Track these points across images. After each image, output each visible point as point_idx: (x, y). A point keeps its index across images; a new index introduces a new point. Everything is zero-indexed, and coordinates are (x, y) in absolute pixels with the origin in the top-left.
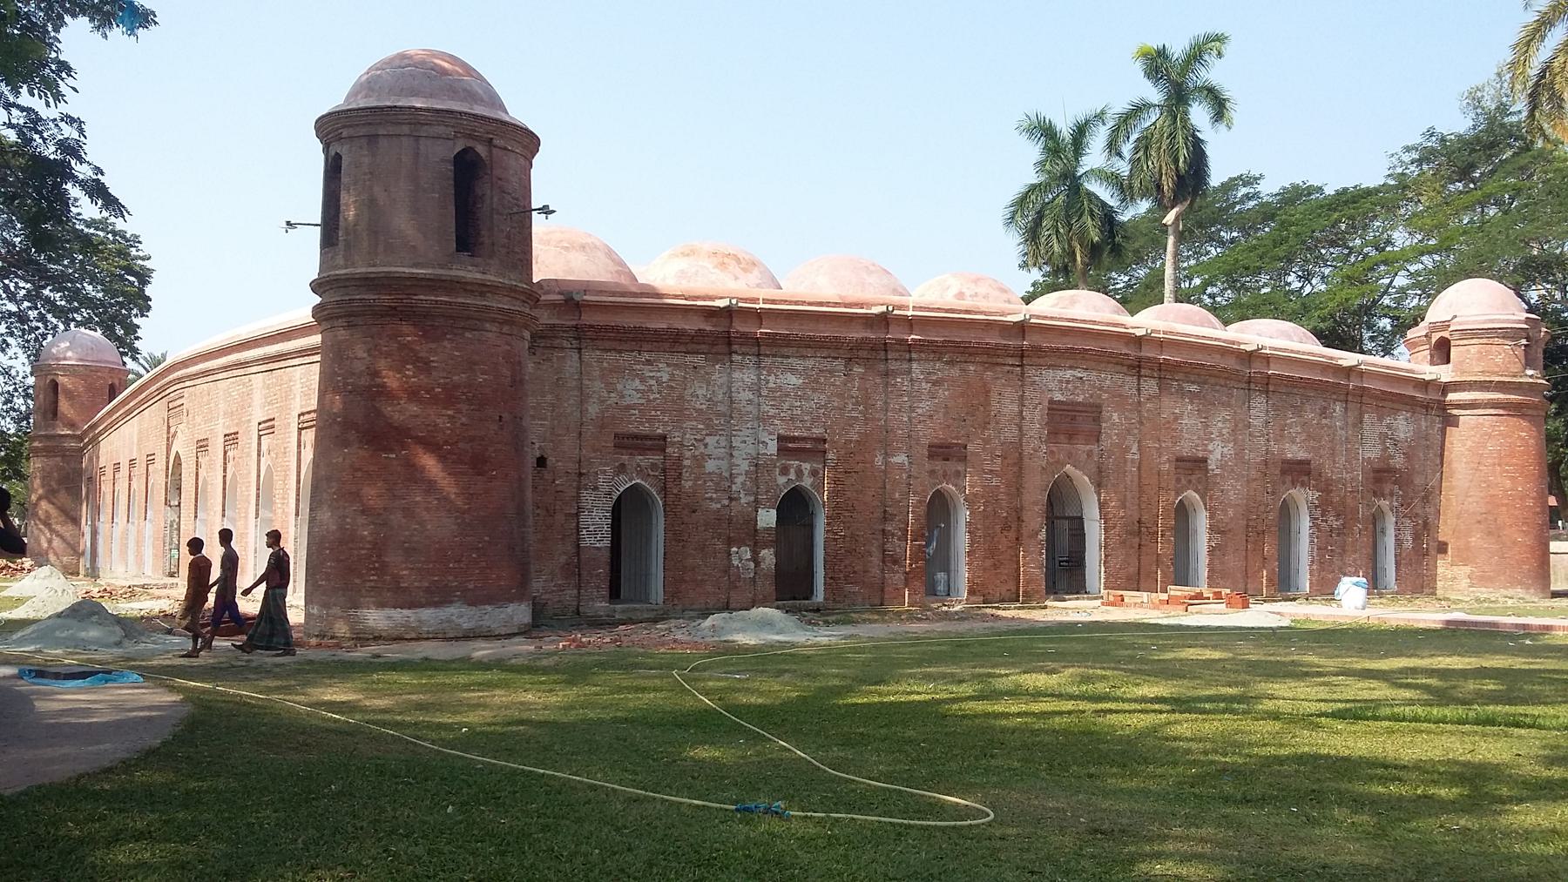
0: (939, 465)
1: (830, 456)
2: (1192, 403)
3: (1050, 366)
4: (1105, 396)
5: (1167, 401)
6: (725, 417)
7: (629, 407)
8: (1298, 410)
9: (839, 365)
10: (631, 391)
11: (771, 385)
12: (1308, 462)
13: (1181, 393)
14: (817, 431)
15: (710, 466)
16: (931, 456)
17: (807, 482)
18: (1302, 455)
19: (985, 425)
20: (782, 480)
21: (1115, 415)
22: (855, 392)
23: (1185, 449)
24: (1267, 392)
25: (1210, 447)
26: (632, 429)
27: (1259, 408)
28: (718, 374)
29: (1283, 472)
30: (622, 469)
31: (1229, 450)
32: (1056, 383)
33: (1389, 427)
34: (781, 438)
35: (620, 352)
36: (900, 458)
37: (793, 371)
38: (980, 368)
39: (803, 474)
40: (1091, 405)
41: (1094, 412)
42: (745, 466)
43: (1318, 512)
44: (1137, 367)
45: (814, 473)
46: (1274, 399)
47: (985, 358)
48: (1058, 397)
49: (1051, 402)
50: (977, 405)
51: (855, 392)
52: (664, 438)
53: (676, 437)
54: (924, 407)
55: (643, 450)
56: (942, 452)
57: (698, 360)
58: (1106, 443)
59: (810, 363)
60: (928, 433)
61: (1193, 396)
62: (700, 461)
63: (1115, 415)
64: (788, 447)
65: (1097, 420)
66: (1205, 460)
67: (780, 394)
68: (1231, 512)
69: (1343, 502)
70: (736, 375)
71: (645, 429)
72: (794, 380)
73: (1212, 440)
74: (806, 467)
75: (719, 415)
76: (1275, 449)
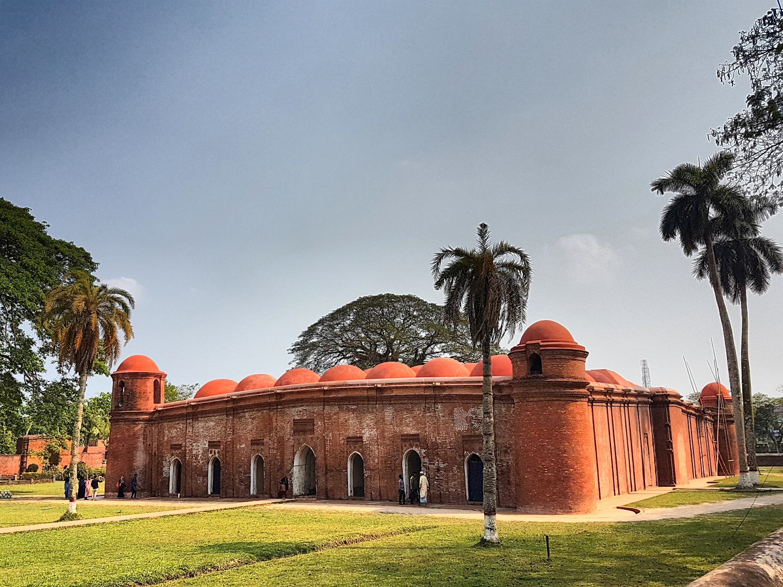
0: (255, 447)
1: (221, 447)
2: (353, 413)
3: (293, 407)
4: (315, 415)
5: (341, 414)
7: (174, 437)
8: (410, 411)
10: (174, 432)
11: (207, 426)
13: (348, 410)
16: (252, 444)
17: (217, 455)
18: (413, 432)
19: (270, 431)
20: (210, 455)
21: (319, 422)
22: (230, 425)
23: (351, 433)
24: (392, 404)
25: (363, 432)
26: (174, 443)
27: (389, 413)
30: (172, 455)
32: (295, 413)
33: (474, 413)
34: (209, 442)
35: (172, 422)
36: (243, 446)
37: (212, 421)
38: (268, 411)
39: (216, 453)
40: (309, 419)
41: (311, 421)
43: (426, 460)
44: (325, 402)
49: (294, 420)
50: (268, 426)
51: (230, 425)
52: (181, 444)
54: (250, 427)
55: (178, 449)
56: (254, 442)
58: (316, 434)
60: (250, 437)
61: (354, 411)
63: (319, 422)
64: (212, 444)
66: (361, 437)
67: (208, 429)
68: (376, 461)
71: (177, 443)
72: (213, 424)
74: (217, 450)
75: (197, 436)
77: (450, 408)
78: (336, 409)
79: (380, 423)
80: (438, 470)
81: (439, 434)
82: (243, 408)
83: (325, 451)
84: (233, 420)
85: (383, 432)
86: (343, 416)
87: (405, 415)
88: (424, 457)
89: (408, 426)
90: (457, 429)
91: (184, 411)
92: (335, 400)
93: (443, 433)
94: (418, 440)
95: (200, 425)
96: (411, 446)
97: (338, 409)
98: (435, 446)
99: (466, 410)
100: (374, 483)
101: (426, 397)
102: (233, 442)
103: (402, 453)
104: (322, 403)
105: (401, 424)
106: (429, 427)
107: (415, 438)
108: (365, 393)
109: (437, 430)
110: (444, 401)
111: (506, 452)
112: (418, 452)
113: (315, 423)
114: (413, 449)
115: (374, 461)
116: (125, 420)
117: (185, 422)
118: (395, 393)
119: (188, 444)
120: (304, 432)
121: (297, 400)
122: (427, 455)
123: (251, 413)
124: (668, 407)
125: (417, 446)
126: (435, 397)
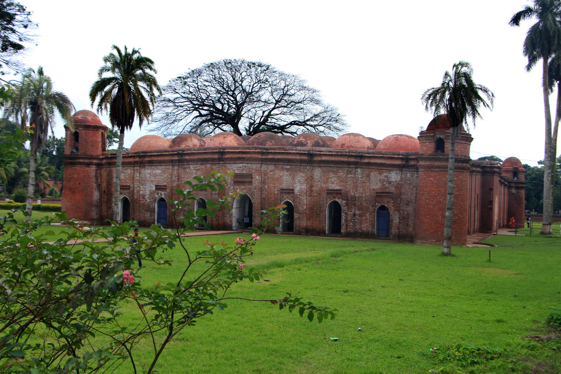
2: (287, 172)
5: (277, 172)
6: (142, 182)
8: (336, 173)
9: (170, 167)
12: (341, 190)
13: (283, 169)
14: (165, 184)
15: (141, 193)
17: (163, 196)
18: (337, 188)
20: (157, 196)
21: (257, 177)
23: (284, 186)
25: (295, 186)
27: (317, 173)
28: (143, 171)
29: (327, 193)
31: (304, 187)
32: (235, 168)
33: (386, 177)
34: (156, 186)
37: (159, 169)
38: (211, 165)
39: (163, 194)
41: (250, 176)
42: (148, 192)
44: (263, 161)
45: (165, 194)
46: (324, 169)
47: (211, 162)
48: (237, 172)
49: (235, 173)
53: (132, 186)
55: (126, 189)
57: (138, 168)
59: (163, 167)
61: (288, 170)
62: (139, 191)
64: (158, 188)
65: (252, 178)
66: (293, 190)
67: (155, 175)
68: (305, 207)
69: (361, 204)
70: (146, 171)
71: (125, 184)
72: (159, 171)
73: (295, 183)
74: (163, 193)
75: (144, 180)
76: (324, 186)
77: (368, 172)
78: (272, 167)
79: (310, 180)
80: (355, 215)
81: (357, 190)
82: (188, 161)
83: (261, 198)
84: (178, 170)
85: (312, 186)
86: (278, 173)
87: (331, 175)
88: (344, 206)
89: (333, 183)
90: (372, 187)
91: (131, 160)
92: (272, 160)
93: (361, 190)
94: (341, 194)
95: (147, 172)
96: (334, 198)
97: (274, 168)
98: (354, 198)
99: (380, 174)
100: (301, 222)
101: (349, 163)
102: (178, 186)
103: (327, 203)
104: (260, 162)
105: (327, 182)
106: (350, 185)
107: (338, 192)
108: (298, 157)
109: (356, 187)
110: (363, 167)
111: (407, 204)
112: (340, 202)
113: (253, 177)
114: (336, 200)
115: (303, 208)
116: (81, 163)
117: (132, 168)
118: (324, 158)
119: (135, 186)
120: (243, 183)
121: (239, 159)
122: (347, 204)
123: (195, 166)
124: (493, 175)
125: (339, 198)
126: (356, 164)
